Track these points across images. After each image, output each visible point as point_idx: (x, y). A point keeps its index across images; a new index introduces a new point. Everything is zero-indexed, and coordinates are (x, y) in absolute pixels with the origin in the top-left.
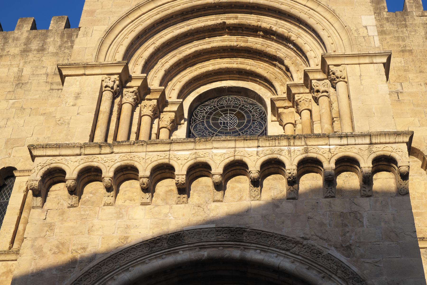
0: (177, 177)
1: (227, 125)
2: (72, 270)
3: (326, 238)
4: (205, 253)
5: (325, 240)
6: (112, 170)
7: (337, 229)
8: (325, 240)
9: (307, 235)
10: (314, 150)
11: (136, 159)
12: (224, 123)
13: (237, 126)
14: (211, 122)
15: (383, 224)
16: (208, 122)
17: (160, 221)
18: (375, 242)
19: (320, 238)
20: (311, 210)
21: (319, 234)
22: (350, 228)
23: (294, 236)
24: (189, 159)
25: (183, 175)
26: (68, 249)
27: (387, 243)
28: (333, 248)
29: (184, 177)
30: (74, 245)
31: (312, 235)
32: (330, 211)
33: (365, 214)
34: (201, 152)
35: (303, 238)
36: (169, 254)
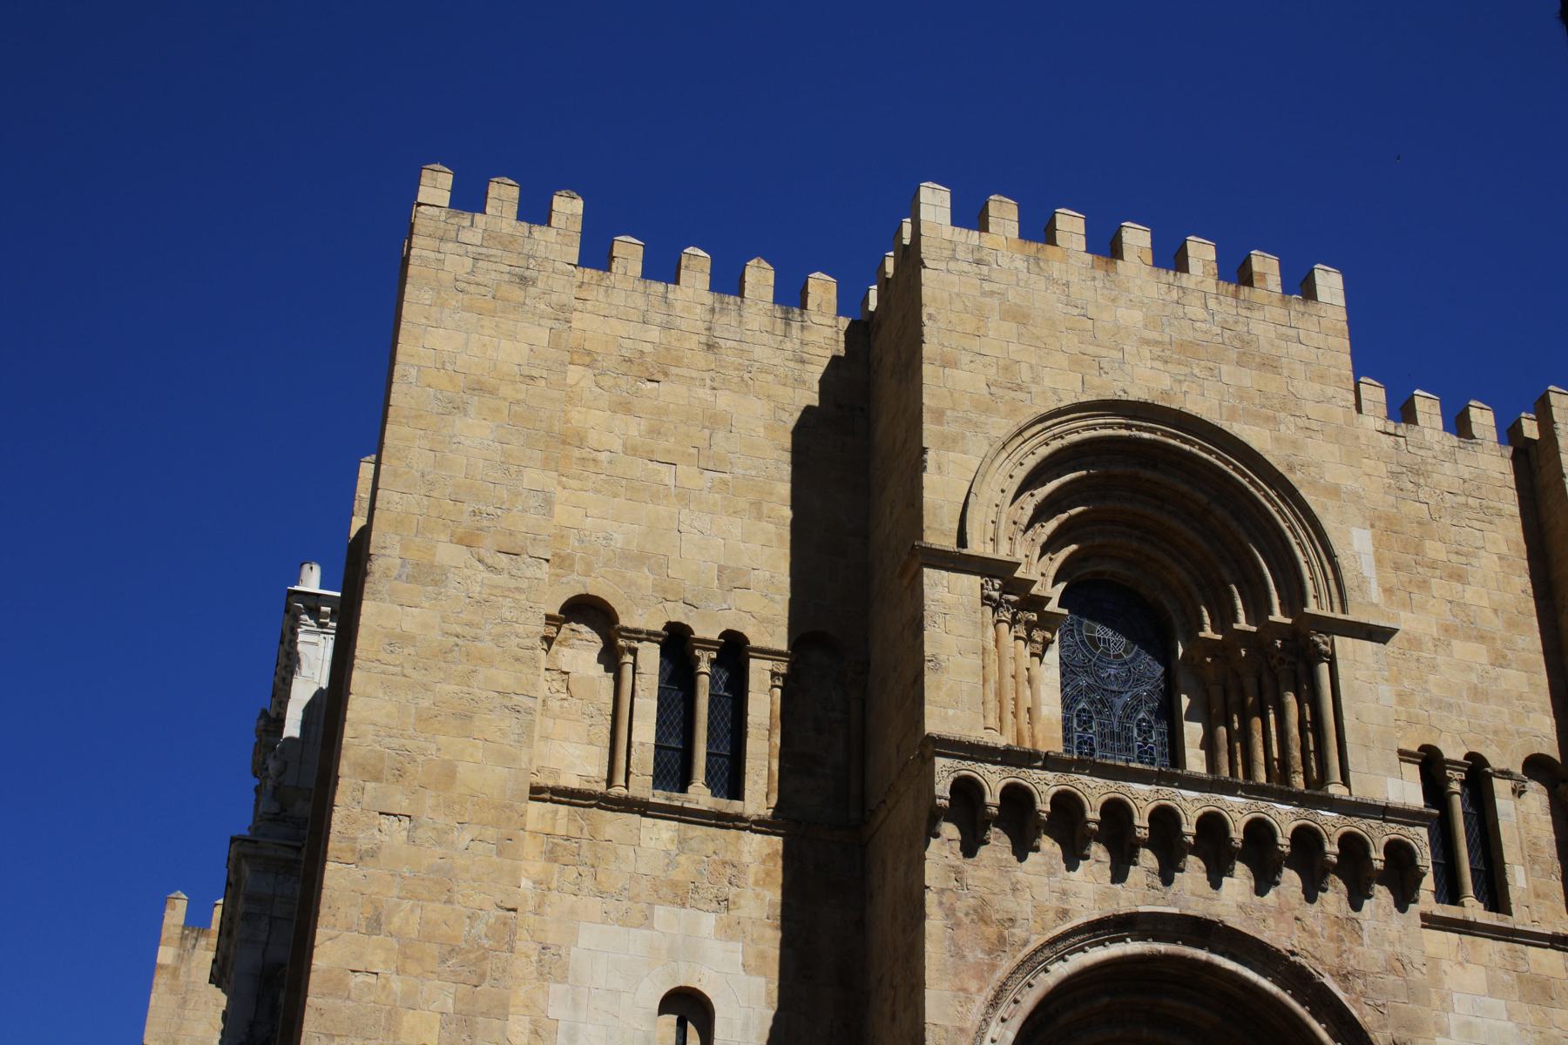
0: (1137, 829)
1: (1109, 645)
2: (1002, 954)
3: (1318, 957)
4: (1162, 947)
5: (1318, 959)
6: (1048, 799)
7: (1331, 944)
8: (1318, 959)
9: (1295, 947)
10: (1311, 816)
11: (1080, 786)
12: (1104, 639)
13: (1123, 651)
14: (1085, 633)
15: (1386, 945)
16: (1080, 633)
17: (1107, 890)
18: (1378, 973)
19: (1313, 956)
20: (1298, 906)
21: (1310, 949)
22: (1348, 944)
23: (1279, 947)
24: (1150, 800)
25: (1145, 828)
26: (991, 916)
27: (1392, 977)
28: (1327, 975)
29: (1147, 832)
30: (998, 911)
31: (1302, 949)
32: (1322, 912)
33: (1365, 925)
34: (1166, 791)
35: (1290, 952)
36: (1113, 941)
